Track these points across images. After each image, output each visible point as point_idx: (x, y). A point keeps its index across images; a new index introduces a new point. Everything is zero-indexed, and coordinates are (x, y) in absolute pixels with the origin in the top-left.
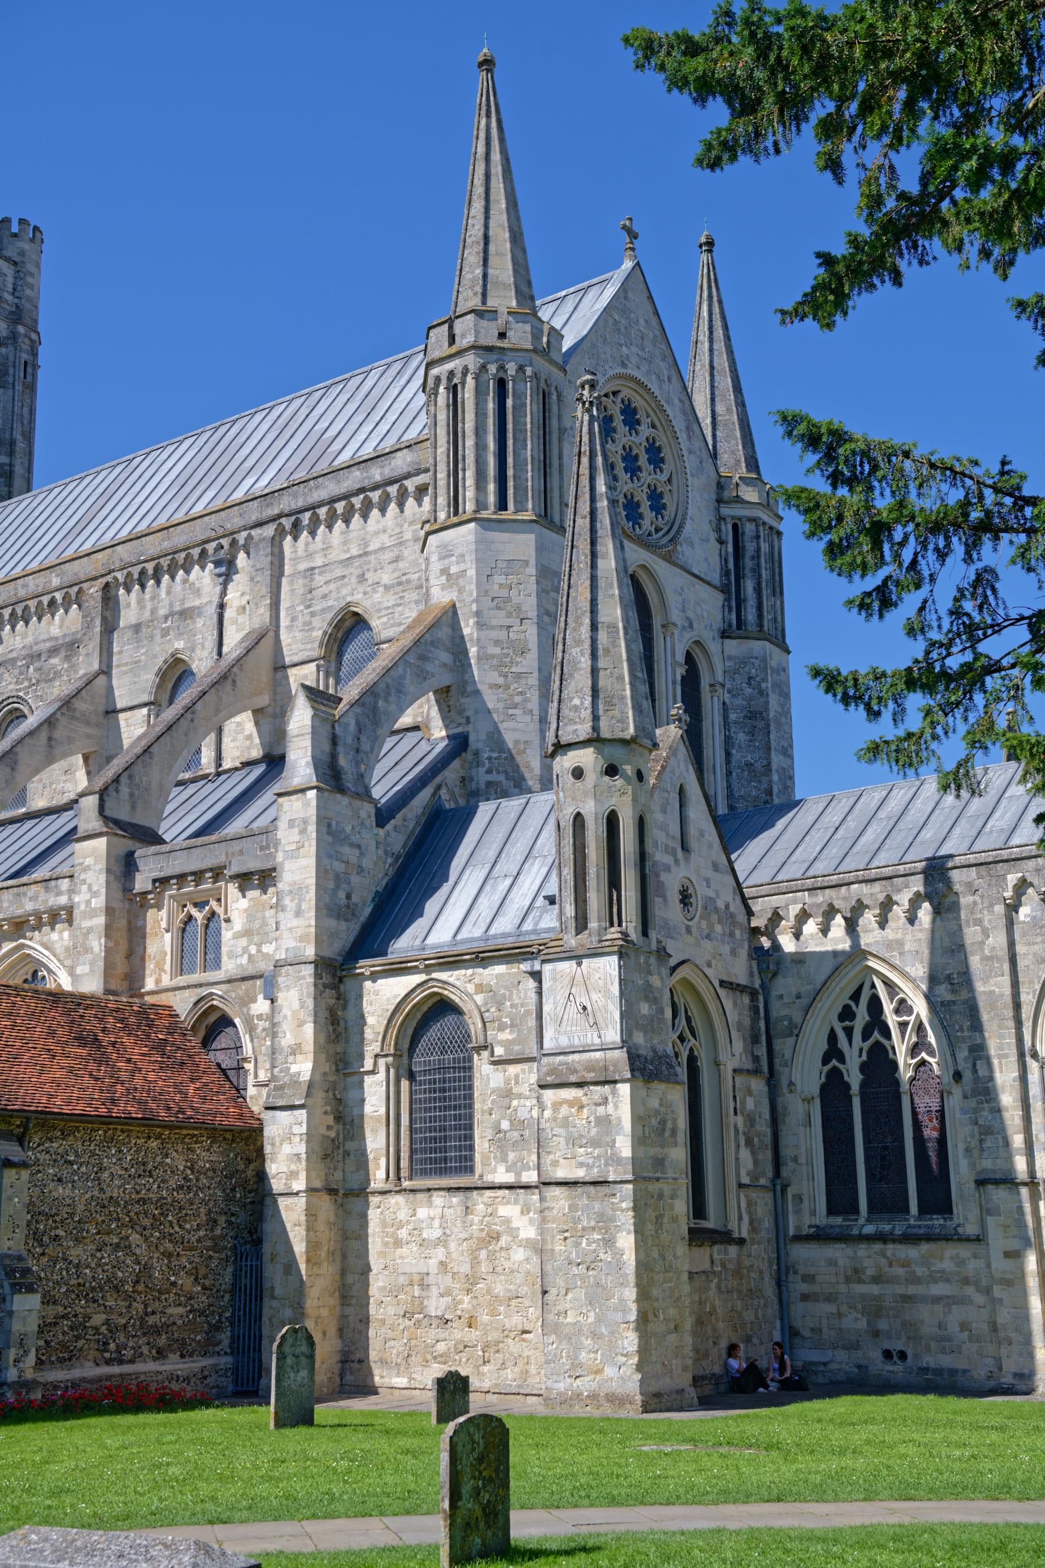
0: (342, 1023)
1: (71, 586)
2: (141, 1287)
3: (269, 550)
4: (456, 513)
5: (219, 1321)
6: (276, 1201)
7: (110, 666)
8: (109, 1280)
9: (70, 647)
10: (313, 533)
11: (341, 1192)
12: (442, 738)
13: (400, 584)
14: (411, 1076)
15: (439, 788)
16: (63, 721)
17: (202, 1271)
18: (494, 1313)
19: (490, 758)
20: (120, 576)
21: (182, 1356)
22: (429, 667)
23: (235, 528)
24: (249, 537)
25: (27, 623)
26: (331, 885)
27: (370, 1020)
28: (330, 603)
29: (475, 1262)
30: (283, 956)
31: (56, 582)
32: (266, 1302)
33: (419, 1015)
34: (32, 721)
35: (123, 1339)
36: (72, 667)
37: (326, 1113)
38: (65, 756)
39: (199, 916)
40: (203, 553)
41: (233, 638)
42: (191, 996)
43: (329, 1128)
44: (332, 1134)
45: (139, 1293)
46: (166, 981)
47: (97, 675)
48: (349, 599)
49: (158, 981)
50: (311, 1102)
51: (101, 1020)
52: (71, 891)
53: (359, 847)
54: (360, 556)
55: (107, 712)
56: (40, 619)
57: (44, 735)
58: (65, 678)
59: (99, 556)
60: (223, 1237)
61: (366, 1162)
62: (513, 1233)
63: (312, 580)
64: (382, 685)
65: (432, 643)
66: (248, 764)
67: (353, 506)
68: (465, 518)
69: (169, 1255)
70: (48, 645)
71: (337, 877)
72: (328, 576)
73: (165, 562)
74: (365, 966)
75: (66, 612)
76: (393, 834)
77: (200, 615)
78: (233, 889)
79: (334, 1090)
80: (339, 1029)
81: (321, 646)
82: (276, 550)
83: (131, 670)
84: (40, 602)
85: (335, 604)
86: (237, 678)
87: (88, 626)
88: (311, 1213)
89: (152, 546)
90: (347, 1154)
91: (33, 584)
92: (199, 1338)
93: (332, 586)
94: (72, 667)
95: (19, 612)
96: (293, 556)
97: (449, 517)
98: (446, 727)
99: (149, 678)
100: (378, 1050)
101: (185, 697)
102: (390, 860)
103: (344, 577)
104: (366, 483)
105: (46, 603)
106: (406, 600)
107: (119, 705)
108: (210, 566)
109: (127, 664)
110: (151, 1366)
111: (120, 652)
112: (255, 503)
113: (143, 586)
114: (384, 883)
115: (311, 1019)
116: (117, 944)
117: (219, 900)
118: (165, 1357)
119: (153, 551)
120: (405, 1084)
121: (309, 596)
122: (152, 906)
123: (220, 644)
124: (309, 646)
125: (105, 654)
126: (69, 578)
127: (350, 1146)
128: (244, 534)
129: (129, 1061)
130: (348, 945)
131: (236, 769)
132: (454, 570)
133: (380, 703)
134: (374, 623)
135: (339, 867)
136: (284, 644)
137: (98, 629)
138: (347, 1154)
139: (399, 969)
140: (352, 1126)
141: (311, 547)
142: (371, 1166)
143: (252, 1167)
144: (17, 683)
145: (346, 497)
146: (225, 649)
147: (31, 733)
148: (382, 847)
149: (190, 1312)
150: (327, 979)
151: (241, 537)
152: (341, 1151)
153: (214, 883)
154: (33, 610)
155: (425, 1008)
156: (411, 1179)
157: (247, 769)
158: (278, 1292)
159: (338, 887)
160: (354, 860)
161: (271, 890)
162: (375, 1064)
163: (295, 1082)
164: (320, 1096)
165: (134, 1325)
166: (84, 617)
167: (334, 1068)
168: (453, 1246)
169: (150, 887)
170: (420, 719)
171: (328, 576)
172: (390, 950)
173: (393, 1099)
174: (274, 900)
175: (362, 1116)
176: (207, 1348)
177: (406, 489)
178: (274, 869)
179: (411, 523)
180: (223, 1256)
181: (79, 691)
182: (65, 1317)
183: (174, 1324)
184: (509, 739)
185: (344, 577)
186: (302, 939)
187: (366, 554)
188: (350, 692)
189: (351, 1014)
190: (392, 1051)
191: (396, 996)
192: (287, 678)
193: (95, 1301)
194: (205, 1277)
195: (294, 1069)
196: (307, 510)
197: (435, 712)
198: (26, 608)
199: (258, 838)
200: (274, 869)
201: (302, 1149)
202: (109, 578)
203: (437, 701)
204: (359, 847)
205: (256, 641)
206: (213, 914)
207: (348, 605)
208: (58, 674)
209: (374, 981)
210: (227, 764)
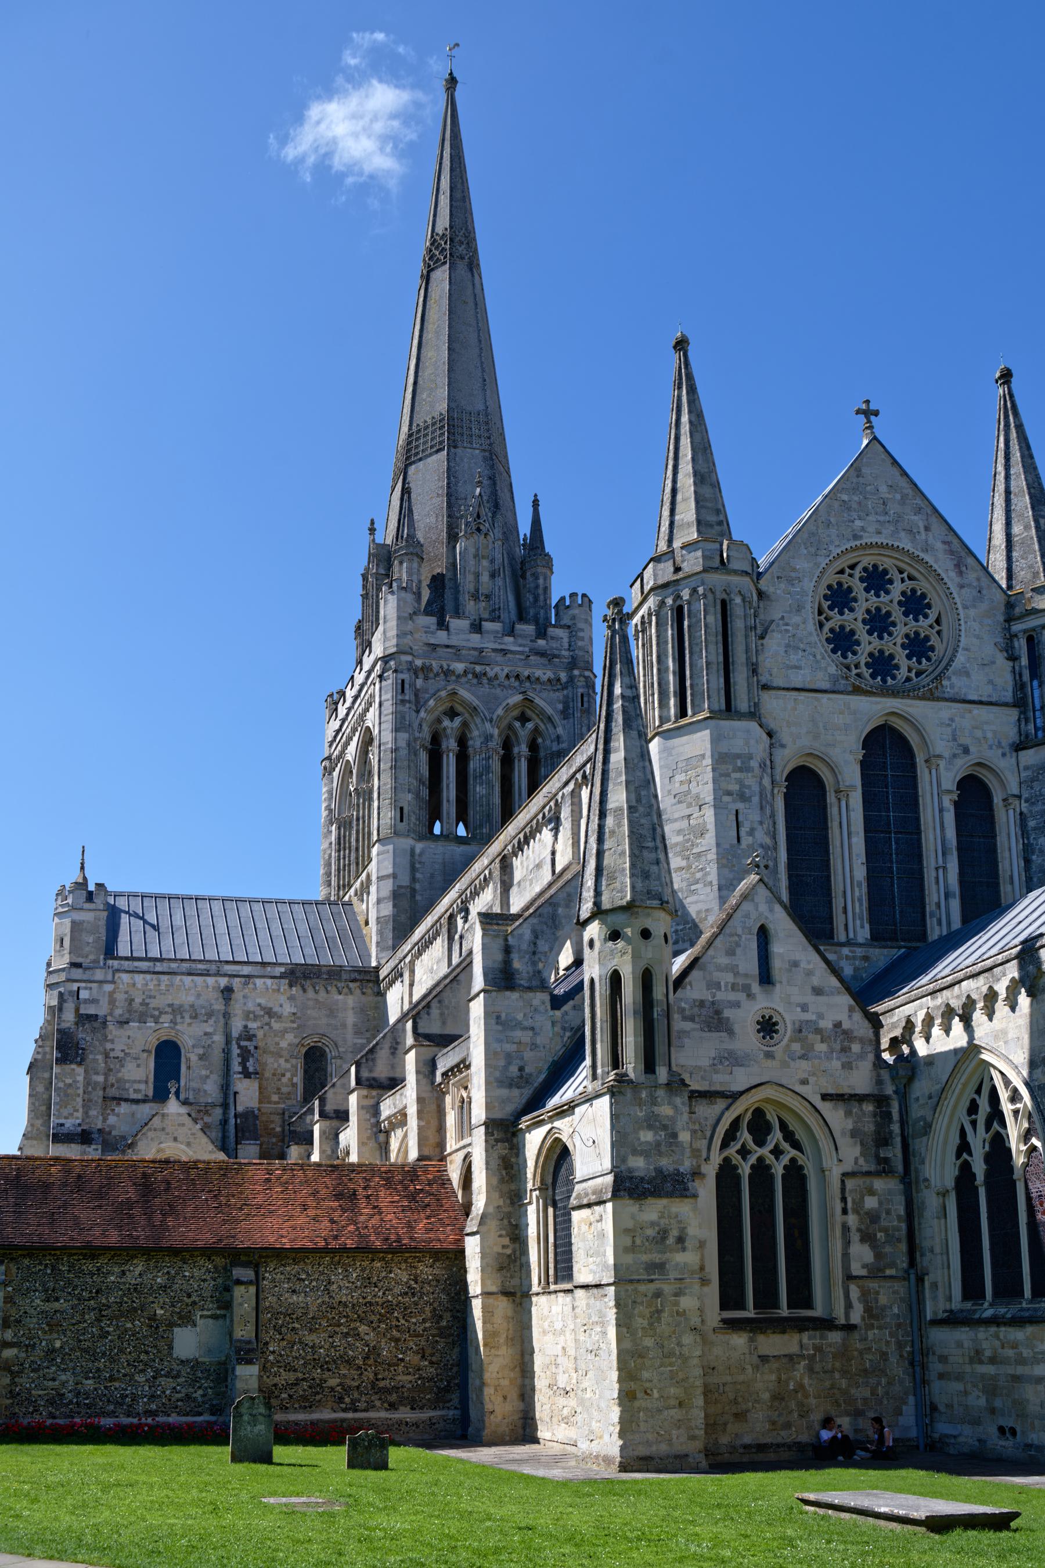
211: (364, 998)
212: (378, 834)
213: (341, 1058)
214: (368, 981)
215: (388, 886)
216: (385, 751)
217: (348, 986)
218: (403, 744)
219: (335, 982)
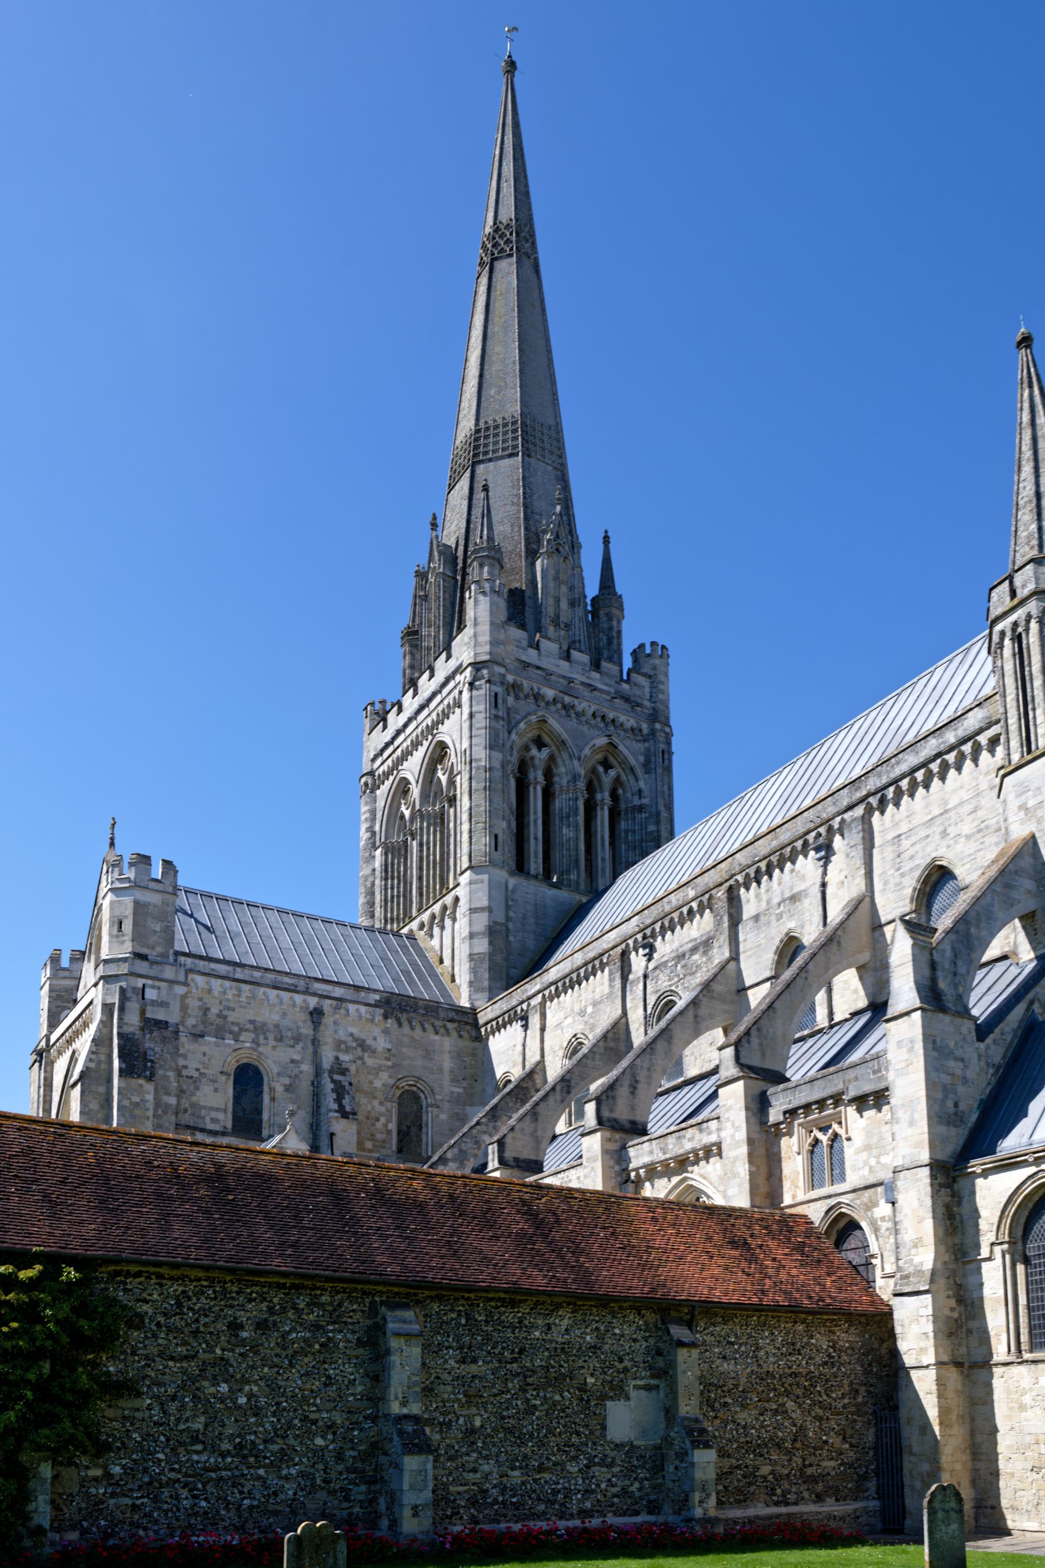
0: (958, 1218)
1: (703, 895)
2: (798, 1445)
3: (860, 827)
4: (1029, 751)
5: (866, 1472)
6: (908, 1374)
7: (737, 953)
8: (771, 1439)
9: (705, 945)
10: (897, 805)
11: (967, 1365)
12: (1031, 960)
13: (979, 831)
15: (1031, 1003)
16: (705, 1001)
17: (849, 1432)
20: (740, 878)
21: (837, 1500)
22: (1015, 894)
23: (830, 815)
24: (843, 821)
25: (673, 932)
26: (939, 1095)
27: (983, 1212)
28: (917, 862)
30: (900, 1163)
31: (691, 893)
32: (906, 1457)
33: (1031, 1205)
34: (680, 1004)
35: (787, 1486)
36: (709, 959)
37: (948, 1297)
38: (708, 1029)
39: (824, 1138)
40: (806, 844)
41: (835, 914)
42: (821, 1207)
43: (952, 1309)
44: (955, 1315)
45: (798, 1449)
46: (801, 1197)
47: (728, 961)
48: (934, 855)
49: (794, 1197)
50: (935, 1288)
51: (749, 1228)
52: (719, 1130)
53: (962, 1060)
54: (942, 814)
55: (739, 991)
56: (682, 927)
57: (691, 1013)
58: (704, 969)
59: (723, 865)
60: (864, 1404)
63: (900, 845)
64: (973, 913)
65: (1016, 872)
66: (855, 1014)
67: (931, 771)
68: (1038, 753)
69: (820, 1419)
70: (690, 945)
71: (945, 1088)
72: (913, 839)
73: (774, 859)
74: (976, 1165)
75: (702, 916)
76: (993, 1047)
77: (806, 896)
78: (851, 1111)
79: (955, 1276)
80: (956, 1223)
81: (911, 902)
82: (866, 827)
83: (754, 954)
84: (681, 913)
85: (922, 862)
86: (842, 940)
87: (718, 923)
88: (940, 1382)
89: (763, 847)
90: (969, 1332)
91: (675, 899)
92: (850, 1486)
93: (918, 847)
94: (709, 959)
95: (667, 924)
96: (882, 828)
97: (1023, 756)
98: (1034, 949)
99: (769, 957)
101: (799, 961)
102: (991, 1071)
103: (928, 836)
104: (942, 748)
105: (685, 912)
106: (987, 844)
107: (748, 984)
108: (812, 853)
109: (750, 949)
110: (812, 1508)
111: (745, 941)
112: (846, 790)
113: (759, 883)
114: (987, 1091)
115: (931, 1215)
116: (758, 1168)
117: (840, 1123)
118: (823, 1501)
119: (764, 852)
121: (898, 860)
122: (785, 1135)
123: (825, 917)
124: (901, 904)
125: (733, 944)
126: (701, 889)
127: (973, 1324)
128: (838, 819)
129: (774, 1260)
130: (959, 1148)
131: (846, 1020)
132: (1031, 803)
133: (973, 930)
134: (957, 871)
135: (946, 1079)
136: (879, 906)
137: (726, 925)
138: (969, 1332)
139: (1010, 1164)
140: (973, 1308)
141: (897, 818)
143: (885, 1345)
144: (670, 980)
145: (924, 765)
146: (829, 920)
147: (681, 1013)
148: (983, 1059)
149: (841, 1464)
150: (941, 1179)
151: (836, 823)
152: (964, 1329)
153: (835, 1108)
154: (676, 920)
155: (1036, 1198)
157: (856, 1018)
158: (916, 1449)
159: (946, 1097)
160: (958, 1072)
161: (885, 1108)
162: (991, 1252)
163: (920, 1272)
164: (942, 1282)
165: (795, 1475)
166: (715, 917)
167: (953, 1257)
169: (781, 1118)
170: (1007, 949)
171: (913, 839)
172: (998, 1149)
174: (889, 1116)
176: (857, 1494)
177: (979, 744)
178: (887, 1089)
179: (987, 773)
180: (866, 1420)
181: (715, 976)
182: (738, 1467)
183: (828, 1474)
185: (928, 836)
186: (917, 1145)
187: (946, 811)
188: (943, 922)
189: (965, 1209)
190: (1007, 1239)
192: (883, 935)
193: (761, 1455)
194: (852, 1436)
195: (917, 1260)
196: (890, 785)
197: (1022, 938)
198: (672, 919)
199: (870, 1064)
200: (887, 1089)
201: (929, 1328)
202: (732, 882)
203: (1024, 927)
204: (962, 1060)
205: (857, 905)
206: (836, 1135)
207: (934, 860)
208: (698, 967)
209: (986, 1178)
210: (837, 1018)
211: (460, 1042)
212: (470, 861)
213: (438, 1107)
214: (467, 1023)
215: (482, 921)
216: (478, 768)
217: (444, 1026)
218: (497, 764)
219: (432, 1020)
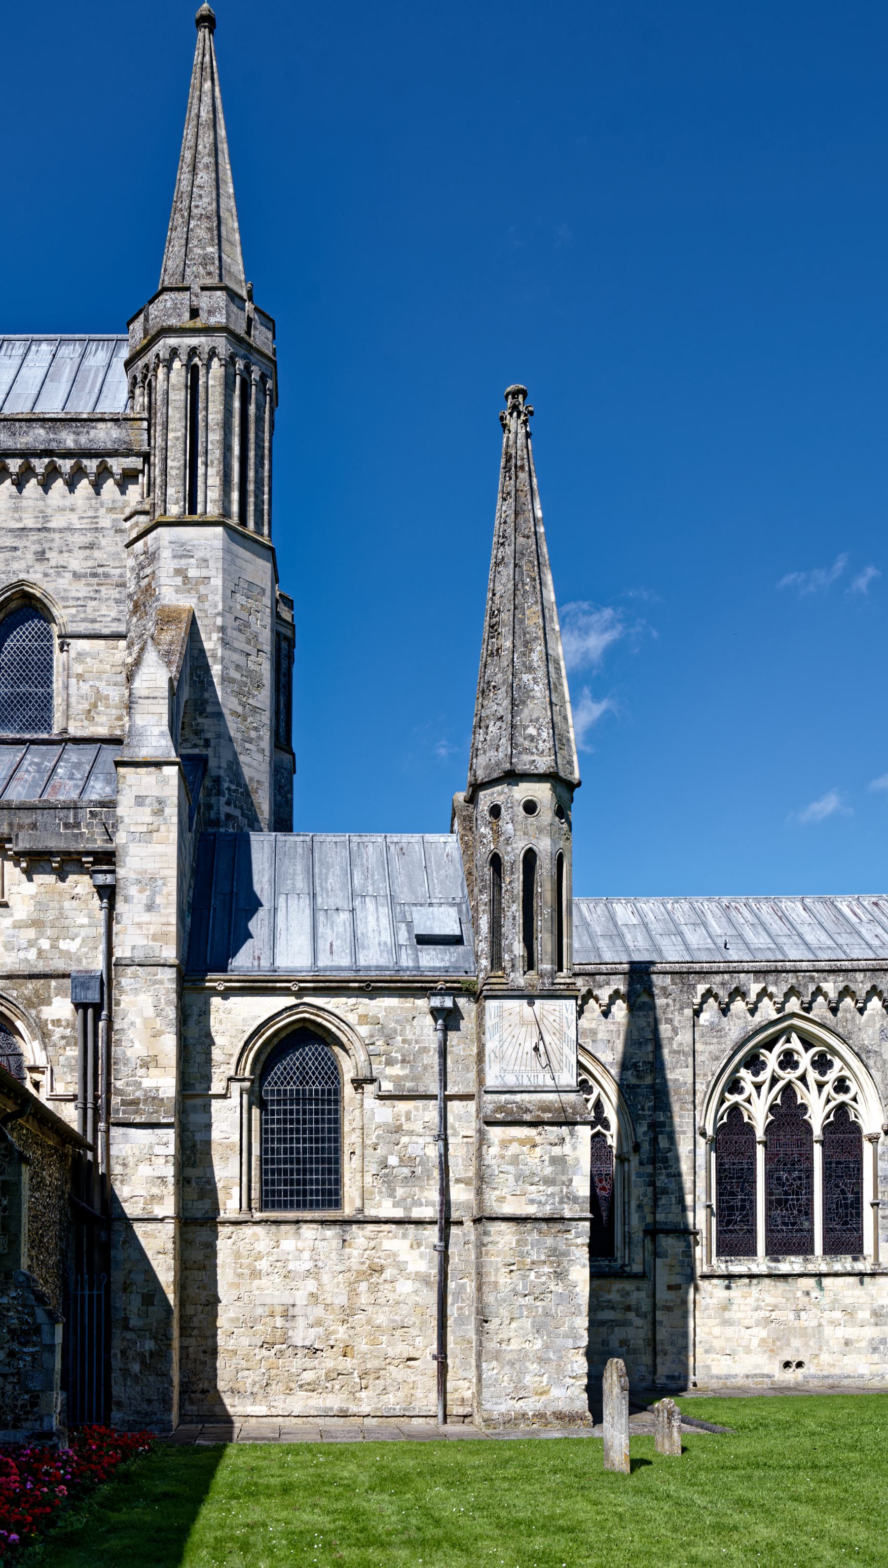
14: (263, 1106)
18: (375, 1342)
19: (229, 789)
29: (353, 1292)
61: (214, 1190)
62: (401, 1267)
100: (232, 1073)
120: (256, 1112)
142: (221, 1195)
156: (261, 1211)
168: (326, 1278)
173: (246, 1127)
175: (208, 1143)
184: (247, 772)
191: (255, 1018)
